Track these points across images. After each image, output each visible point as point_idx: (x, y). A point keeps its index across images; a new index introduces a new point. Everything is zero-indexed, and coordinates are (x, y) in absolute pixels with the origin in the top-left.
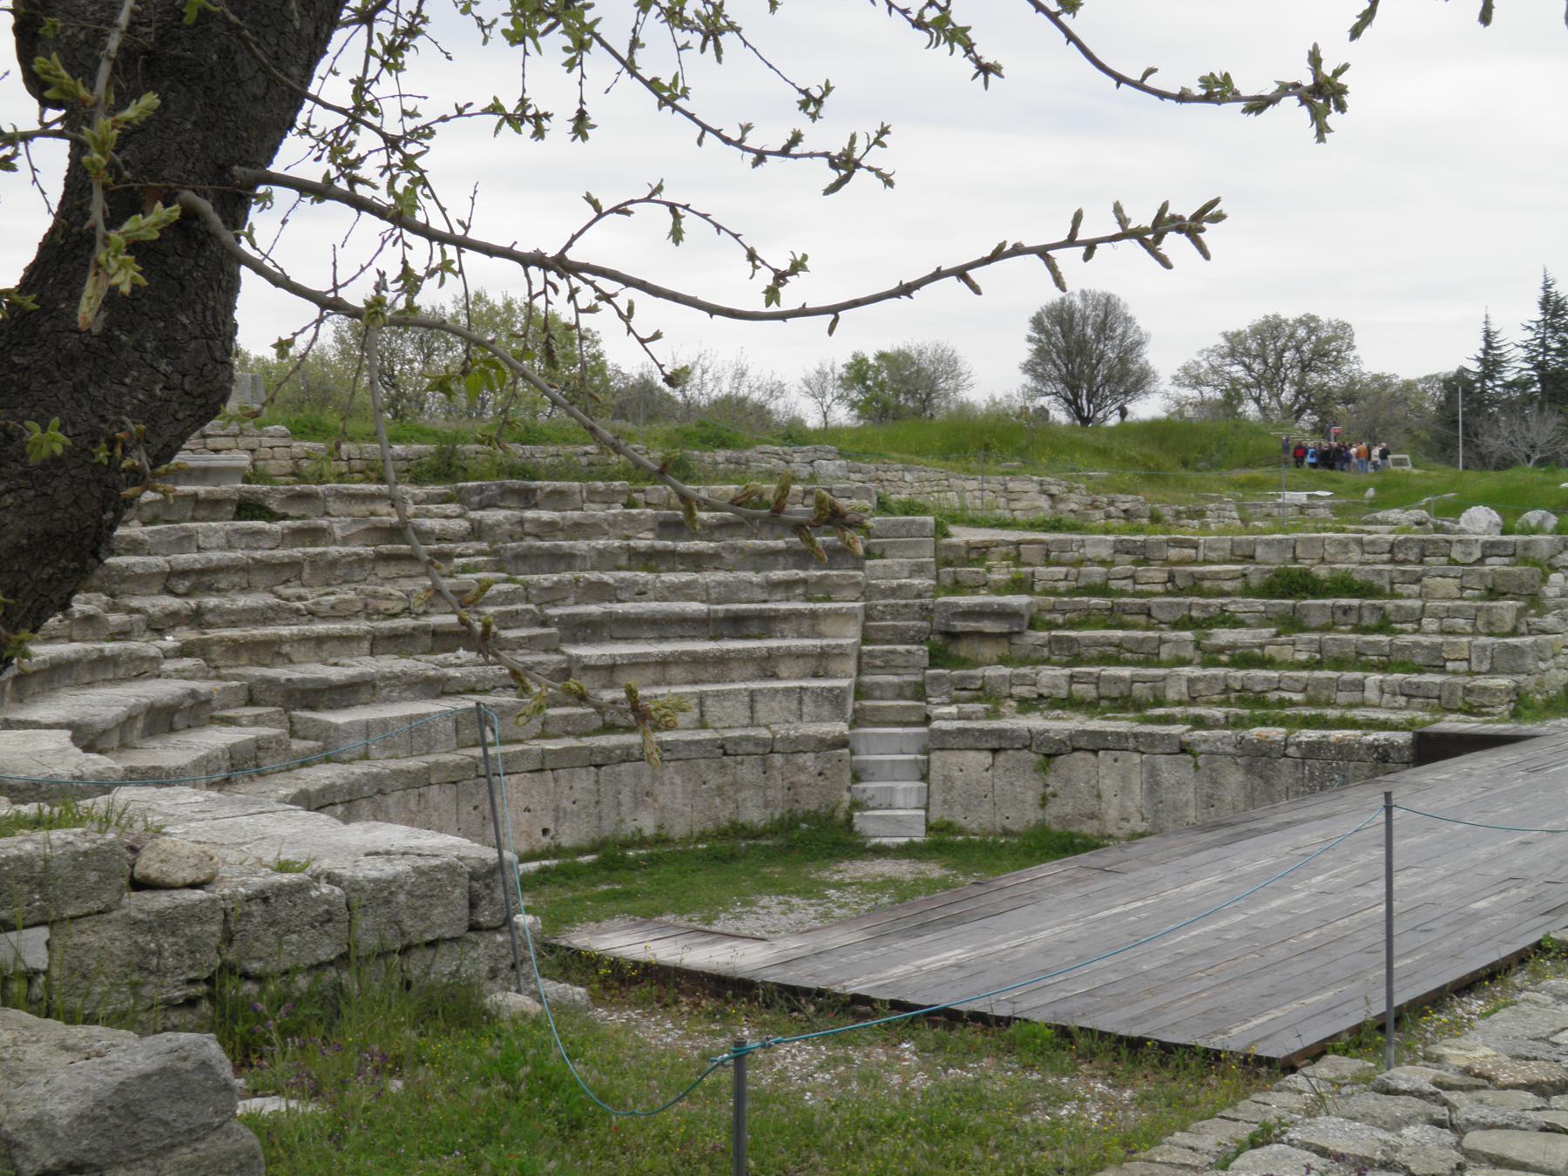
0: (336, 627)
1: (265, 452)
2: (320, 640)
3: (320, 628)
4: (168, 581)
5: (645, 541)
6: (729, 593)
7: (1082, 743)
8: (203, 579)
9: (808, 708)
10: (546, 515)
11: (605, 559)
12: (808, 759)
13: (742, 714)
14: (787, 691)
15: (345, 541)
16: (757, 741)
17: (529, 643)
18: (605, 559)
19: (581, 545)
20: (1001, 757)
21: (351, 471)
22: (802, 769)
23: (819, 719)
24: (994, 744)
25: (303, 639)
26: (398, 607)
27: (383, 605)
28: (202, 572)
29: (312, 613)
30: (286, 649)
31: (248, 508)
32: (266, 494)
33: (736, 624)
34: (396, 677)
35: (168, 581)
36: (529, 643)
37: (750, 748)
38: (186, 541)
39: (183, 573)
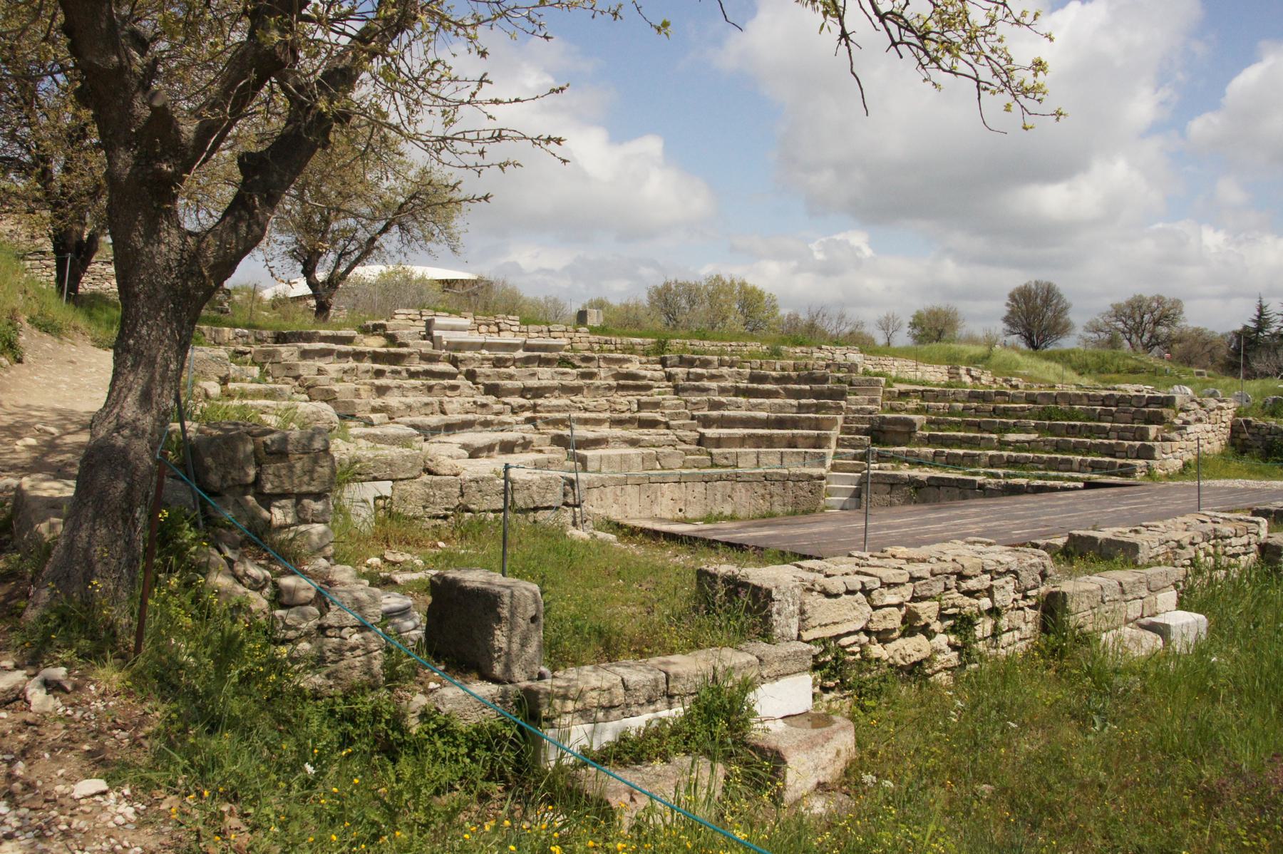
1: (576, 339)
4: (523, 392)
5: (743, 384)
6: (781, 408)
7: (932, 482)
8: (538, 392)
9: (808, 460)
10: (699, 370)
11: (723, 391)
12: (804, 484)
13: (777, 462)
14: (798, 453)
15: (605, 378)
16: (781, 475)
17: (683, 427)
18: (723, 391)
19: (714, 385)
22: (801, 489)
23: (812, 466)
26: (625, 408)
27: (618, 407)
28: (537, 389)
31: (564, 362)
33: (780, 423)
35: (523, 392)
36: (683, 427)
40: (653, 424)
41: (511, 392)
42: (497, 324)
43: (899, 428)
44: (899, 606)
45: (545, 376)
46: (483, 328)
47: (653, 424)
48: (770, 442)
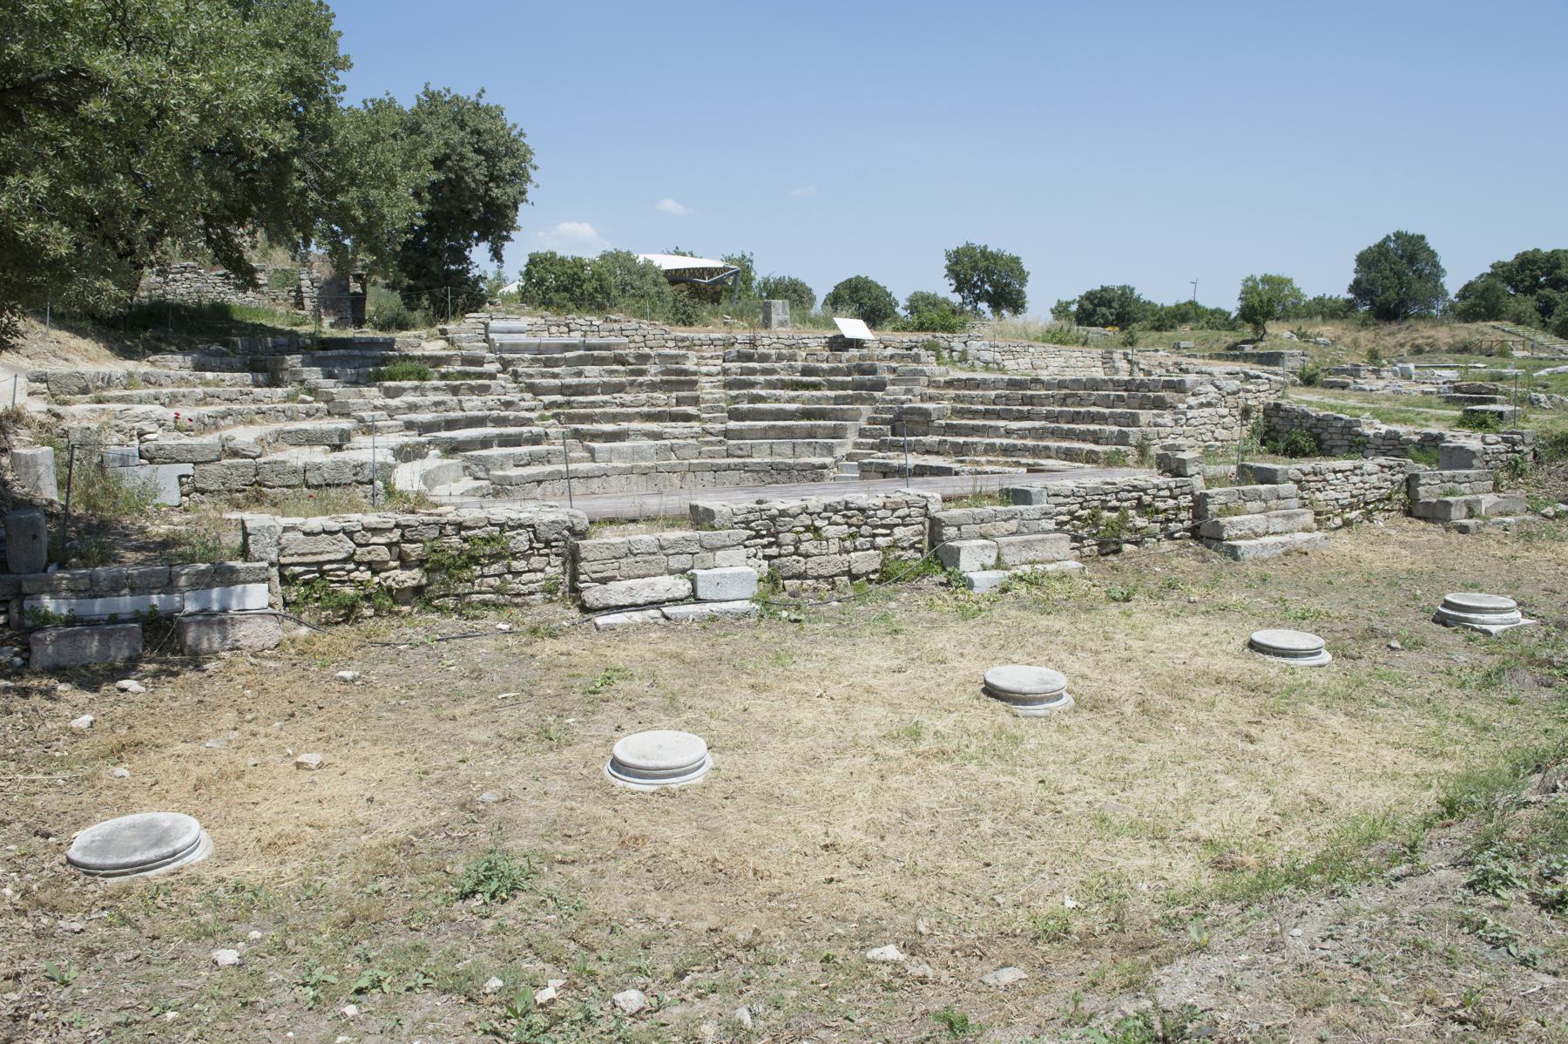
4: (562, 390)
5: (797, 377)
11: (771, 385)
13: (790, 452)
19: (760, 378)
23: (822, 455)
31: (621, 360)
33: (807, 414)
35: (562, 390)
38: (579, 374)
39: (569, 387)
40: (687, 418)
42: (567, 325)
43: (916, 418)
44: (389, 545)
45: (593, 374)
46: (553, 330)
47: (687, 418)
48: (789, 433)
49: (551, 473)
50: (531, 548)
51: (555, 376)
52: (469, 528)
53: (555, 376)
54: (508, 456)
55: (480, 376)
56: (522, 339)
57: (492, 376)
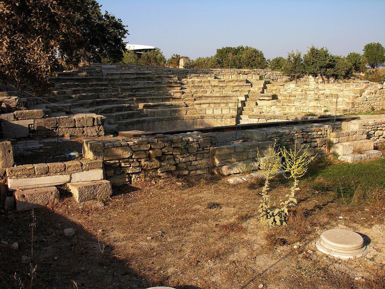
0: (155, 97)
2: (153, 99)
3: (153, 97)
4: (131, 90)
7: (272, 117)
8: (138, 89)
20: (260, 120)
21: (173, 73)
22: (227, 121)
24: (258, 118)
25: (150, 99)
29: (154, 95)
30: (147, 100)
31: (149, 79)
32: (153, 77)
34: (163, 104)
37: (219, 117)
41: (127, 90)
49: (137, 121)
50: (198, 151)
51: (128, 85)
52: (174, 143)
53: (128, 85)
54: (121, 115)
55: (102, 85)
56: (115, 72)
57: (106, 85)
